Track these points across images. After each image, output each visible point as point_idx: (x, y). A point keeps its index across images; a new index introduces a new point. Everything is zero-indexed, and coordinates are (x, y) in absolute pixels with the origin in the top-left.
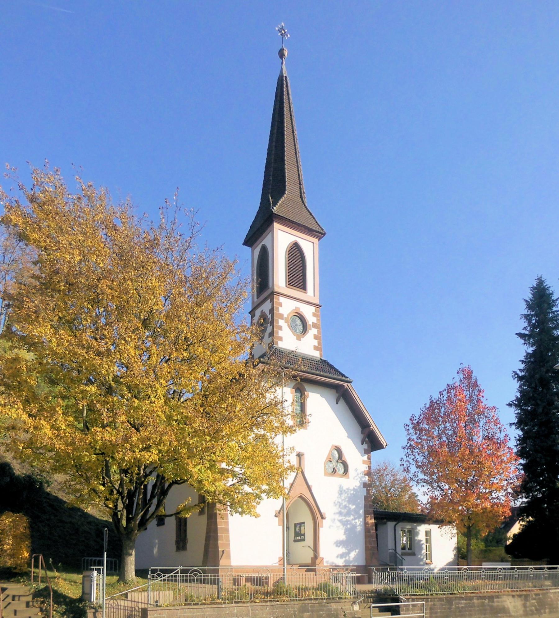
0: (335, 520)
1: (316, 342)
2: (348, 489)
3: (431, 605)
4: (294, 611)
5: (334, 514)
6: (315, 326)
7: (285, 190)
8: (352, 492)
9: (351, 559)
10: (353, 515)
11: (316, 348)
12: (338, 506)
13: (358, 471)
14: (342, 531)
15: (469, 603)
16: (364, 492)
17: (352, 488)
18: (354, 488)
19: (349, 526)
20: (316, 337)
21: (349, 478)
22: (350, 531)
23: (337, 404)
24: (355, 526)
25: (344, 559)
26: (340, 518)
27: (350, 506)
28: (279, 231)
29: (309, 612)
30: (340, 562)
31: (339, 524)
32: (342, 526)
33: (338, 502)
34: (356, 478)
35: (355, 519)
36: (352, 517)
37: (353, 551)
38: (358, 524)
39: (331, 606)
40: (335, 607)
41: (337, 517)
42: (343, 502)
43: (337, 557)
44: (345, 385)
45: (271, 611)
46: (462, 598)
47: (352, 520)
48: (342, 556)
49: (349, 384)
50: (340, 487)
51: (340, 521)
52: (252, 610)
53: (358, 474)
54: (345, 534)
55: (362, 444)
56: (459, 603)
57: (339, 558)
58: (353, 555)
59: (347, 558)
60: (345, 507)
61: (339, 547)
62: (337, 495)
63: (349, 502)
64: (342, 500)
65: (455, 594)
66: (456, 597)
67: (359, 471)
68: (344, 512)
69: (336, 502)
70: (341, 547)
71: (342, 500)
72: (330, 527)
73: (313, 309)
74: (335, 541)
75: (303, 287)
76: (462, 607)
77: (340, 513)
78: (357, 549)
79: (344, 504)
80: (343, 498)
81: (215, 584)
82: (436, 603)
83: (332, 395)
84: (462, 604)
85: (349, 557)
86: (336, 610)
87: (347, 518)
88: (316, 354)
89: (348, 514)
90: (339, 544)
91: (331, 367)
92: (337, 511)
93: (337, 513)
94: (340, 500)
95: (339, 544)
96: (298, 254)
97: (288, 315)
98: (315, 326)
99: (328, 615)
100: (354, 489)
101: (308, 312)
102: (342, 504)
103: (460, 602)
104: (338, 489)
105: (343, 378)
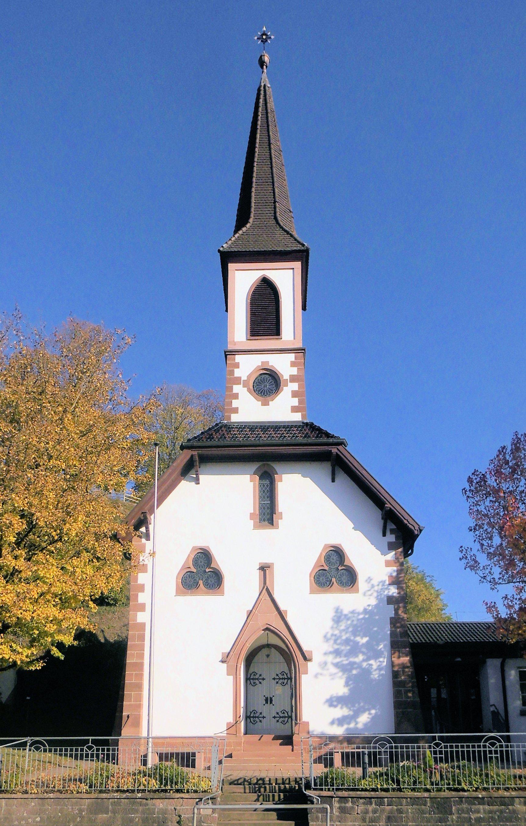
0: (325, 663)
1: (295, 402)
2: (353, 612)
3: (391, 812)
4: (81, 811)
5: (325, 654)
6: (293, 379)
7: (249, 217)
8: (361, 616)
9: (360, 726)
10: (363, 653)
11: (294, 409)
12: (332, 642)
13: (372, 582)
14: (342, 682)
15: (501, 812)
16: (390, 611)
17: (361, 609)
18: (365, 610)
19: (354, 672)
20: (295, 394)
21: (312, 592)
22: (358, 682)
23: (333, 481)
24: (367, 672)
25: (345, 726)
26: (338, 660)
27: (358, 639)
28: (236, 271)
29: (107, 813)
30: (339, 731)
31: (333, 670)
32: (340, 674)
33: (332, 635)
34: (370, 593)
35: (368, 659)
36: (361, 657)
37: (364, 711)
38: (375, 667)
39: (154, 805)
40: (161, 806)
41: (330, 659)
42: (343, 633)
43: (332, 723)
44: (334, 450)
45: (38, 807)
46: (481, 801)
47: (364, 660)
48: (341, 721)
49: (340, 447)
50: (336, 612)
51: (336, 665)
52: (6, 805)
53: (373, 586)
54: (347, 684)
55: (384, 535)
56: (469, 811)
57: (335, 726)
58: (364, 718)
59: (352, 725)
60: (347, 642)
61: (335, 706)
62: (330, 623)
63: (355, 633)
64: (341, 632)
65: (463, 790)
66: (461, 798)
67: (375, 582)
68: (344, 649)
69: (329, 636)
70: (340, 706)
71: (341, 632)
72: (316, 676)
73: (291, 357)
74: (328, 697)
75: (277, 332)
76: (479, 820)
77: (337, 653)
78: (374, 708)
79: (344, 637)
80: (342, 628)
81: (359, 766)
82: (404, 808)
83: (323, 470)
84: (478, 812)
85: (357, 723)
86: (164, 812)
87: (352, 660)
88: (297, 417)
89: (355, 649)
90: (333, 702)
91: (320, 430)
92: (331, 649)
93: (331, 653)
94: (337, 632)
95: (333, 702)
96: (269, 290)
97: (249, 377)
98: (238, 381)
99: (145, 820)
100: (365, 611)
101: (284, 365)
102: (340, 637)
103: (474, 807)
104: (332, 614)
105: (331, 440)
